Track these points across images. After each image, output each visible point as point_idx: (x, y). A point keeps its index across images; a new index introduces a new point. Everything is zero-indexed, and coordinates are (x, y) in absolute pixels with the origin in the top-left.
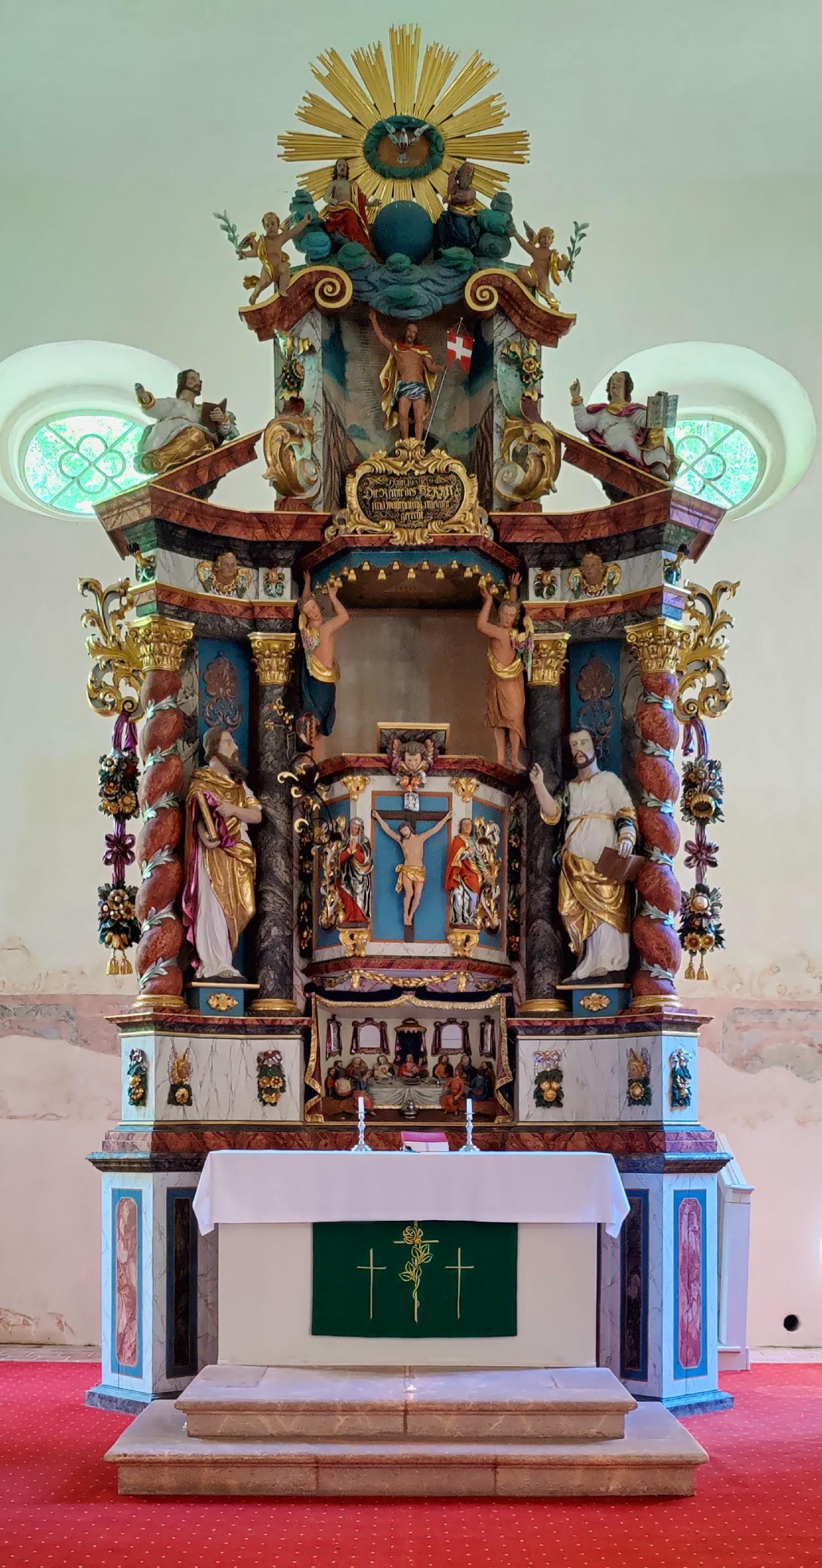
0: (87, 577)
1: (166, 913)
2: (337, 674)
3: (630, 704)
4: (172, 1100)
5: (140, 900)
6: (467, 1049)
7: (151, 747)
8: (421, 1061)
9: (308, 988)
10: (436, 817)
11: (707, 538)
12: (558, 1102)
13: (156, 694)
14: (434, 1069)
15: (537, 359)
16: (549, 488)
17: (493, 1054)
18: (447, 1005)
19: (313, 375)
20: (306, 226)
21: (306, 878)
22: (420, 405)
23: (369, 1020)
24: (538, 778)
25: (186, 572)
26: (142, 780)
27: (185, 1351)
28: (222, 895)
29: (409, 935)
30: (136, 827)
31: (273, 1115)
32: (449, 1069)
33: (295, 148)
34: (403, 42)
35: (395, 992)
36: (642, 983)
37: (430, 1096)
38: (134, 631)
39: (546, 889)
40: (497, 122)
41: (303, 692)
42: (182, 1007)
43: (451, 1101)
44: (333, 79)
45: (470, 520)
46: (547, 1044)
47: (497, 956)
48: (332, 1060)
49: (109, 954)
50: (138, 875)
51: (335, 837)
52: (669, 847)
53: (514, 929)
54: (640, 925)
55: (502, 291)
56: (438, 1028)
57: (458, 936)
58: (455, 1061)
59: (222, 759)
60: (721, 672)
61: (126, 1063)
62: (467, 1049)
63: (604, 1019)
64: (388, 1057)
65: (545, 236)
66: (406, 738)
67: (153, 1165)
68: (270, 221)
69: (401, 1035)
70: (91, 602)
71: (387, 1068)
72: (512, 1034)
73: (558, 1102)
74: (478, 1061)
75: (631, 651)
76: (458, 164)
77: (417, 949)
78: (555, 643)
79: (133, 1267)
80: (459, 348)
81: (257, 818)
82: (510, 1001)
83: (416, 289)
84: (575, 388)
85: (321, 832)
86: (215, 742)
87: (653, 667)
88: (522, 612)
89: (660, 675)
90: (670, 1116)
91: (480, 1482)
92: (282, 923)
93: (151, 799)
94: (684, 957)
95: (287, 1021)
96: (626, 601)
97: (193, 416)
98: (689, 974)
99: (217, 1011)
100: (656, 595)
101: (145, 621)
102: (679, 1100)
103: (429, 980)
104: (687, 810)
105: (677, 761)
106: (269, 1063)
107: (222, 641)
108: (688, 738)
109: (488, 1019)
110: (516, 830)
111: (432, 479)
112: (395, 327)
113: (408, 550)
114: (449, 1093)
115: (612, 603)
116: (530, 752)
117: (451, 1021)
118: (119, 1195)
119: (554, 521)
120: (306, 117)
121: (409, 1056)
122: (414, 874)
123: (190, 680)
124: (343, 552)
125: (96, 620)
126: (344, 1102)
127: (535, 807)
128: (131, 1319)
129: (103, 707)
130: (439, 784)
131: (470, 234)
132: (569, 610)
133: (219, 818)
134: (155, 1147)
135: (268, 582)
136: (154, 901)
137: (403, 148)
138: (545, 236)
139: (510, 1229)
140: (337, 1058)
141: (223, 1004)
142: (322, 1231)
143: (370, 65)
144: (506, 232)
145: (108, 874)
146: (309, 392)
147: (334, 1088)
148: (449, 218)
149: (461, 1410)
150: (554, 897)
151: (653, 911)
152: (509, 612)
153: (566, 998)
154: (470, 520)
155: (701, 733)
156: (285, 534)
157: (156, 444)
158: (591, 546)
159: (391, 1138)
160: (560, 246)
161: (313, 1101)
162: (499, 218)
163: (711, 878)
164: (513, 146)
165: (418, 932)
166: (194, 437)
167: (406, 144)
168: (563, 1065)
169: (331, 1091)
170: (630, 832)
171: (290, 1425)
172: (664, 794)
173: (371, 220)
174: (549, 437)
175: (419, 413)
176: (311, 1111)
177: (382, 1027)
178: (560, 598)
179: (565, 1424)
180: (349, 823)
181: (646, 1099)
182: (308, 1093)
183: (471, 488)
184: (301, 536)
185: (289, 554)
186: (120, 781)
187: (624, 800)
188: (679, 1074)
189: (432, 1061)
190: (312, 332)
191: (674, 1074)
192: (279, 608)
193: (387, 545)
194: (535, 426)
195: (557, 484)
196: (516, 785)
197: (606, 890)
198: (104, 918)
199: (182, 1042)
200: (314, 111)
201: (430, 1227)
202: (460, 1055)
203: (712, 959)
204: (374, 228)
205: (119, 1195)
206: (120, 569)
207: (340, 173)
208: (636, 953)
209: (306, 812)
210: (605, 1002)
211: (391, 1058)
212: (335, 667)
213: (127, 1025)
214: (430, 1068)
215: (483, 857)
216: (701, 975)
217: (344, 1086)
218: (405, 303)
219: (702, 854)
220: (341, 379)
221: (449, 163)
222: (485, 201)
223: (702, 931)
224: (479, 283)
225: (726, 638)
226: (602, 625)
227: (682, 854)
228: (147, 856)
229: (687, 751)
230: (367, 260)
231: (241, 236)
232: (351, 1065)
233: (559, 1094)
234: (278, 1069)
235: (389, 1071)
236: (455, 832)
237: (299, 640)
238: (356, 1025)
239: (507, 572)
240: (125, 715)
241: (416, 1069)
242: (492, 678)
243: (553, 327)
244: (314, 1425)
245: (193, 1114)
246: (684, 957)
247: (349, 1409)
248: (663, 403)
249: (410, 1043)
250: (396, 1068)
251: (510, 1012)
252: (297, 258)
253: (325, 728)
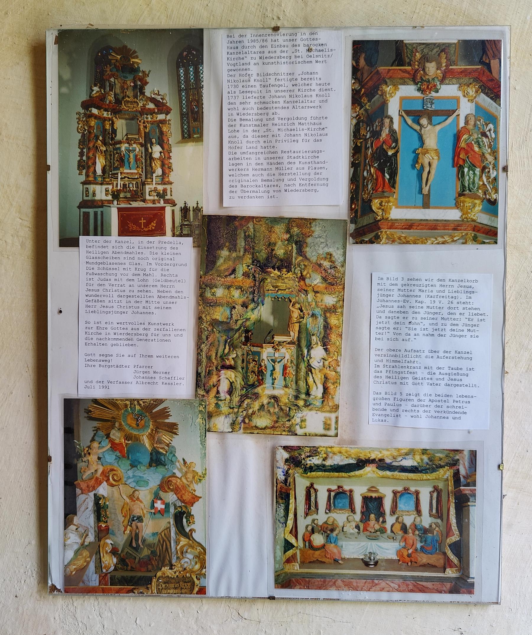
8: (381, 519)
14: (392, 526)
37: (387, 549)
43: (405, 554)
48: (309, 519)
64: (355, 516)
71: (354, 524)
114: (404, 548)
121: (372, 516)
126: (317, 553)
140: (315, 516)
147: (310, 542)
159: (355, 584)
161: (290, 553)
202: (413, 517)
211: (358, 517)
214: (388, 526)
217: (318, 540)
232: (326, 523)
235: (356, 527)
241: (377, 527)
250: (362, 526)
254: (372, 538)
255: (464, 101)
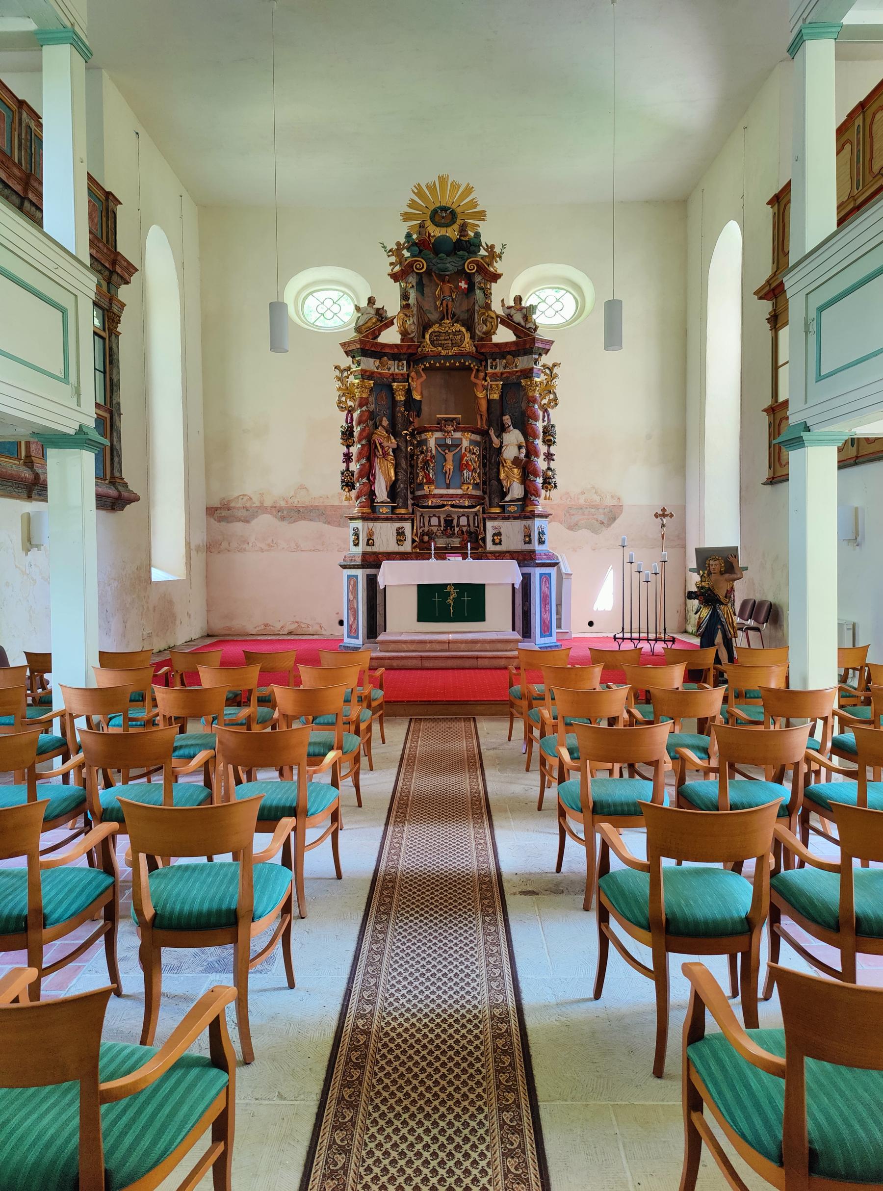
0: (336, 364)
1: (365, 480)
2: (422, 397)
3: (523, 405)
4: (368, 544)
5: (356, 475)
6: (469, 525)
7: (359, 424)
9: (413, 505)
10: (458, 446)
11: (549, 350)
12: (500, 543)
13: (361, 406)
15: (490, 289)
16: (494, 333)
17: (478, 527)
18: (462, 510)
19: (413, 294)
20: (411, 244)
21: (412, 466)
22: (450, 303)
23: (434, 515)
24: (492, 432)
25: (370, 364)
26: (356, 434)
27: (373, 630)
28: (384, 474)
29: (448, 487)
30: (354, 450)
31: (402, 549)
32: (462, 532)
33: (406, 217)
34: (443, 180)
35: (443, 506)
36: (528, 502)
37: (456, 542)
38: (354, 384)
39: (495, 470)
40: (475, 208)
41: (411, 404)
42: (371, 513)
44: (419, 193)
45: (468, 345)
46: (496, 523)
47: (478, 493)
49: (345, 493)
50: (354, 467)
51: (422, 453)
52: (537, 456)
53: (484, 483)
54: (527, 482)
55: (478, 265)
56: (459, 518)
57: (465, 487)
58: (464, 529)
59: (383, 427)
60: (555, 394)
61: (352, 532)
62: (469, 525)
63: (517, 515)
65: (493, 247)
66: (446, 420)
67: (362, 567)
68: (398, 244)
69: (445, 520)
70: (338, 373)
72: (484, 520)
73: (500, 543)
74: (473, 529)
75: (524, 389)
76: (462, 222)
77: (451, 491)
78: (497, 385)
79: (355, 601)
80: (463, 285)
81: (395, 446)
82: (483, 508)
83: (448, 265)
84: (503, 301)
85: (417, 451)
86: (381, 421)
87: (531, 394)
88: (486, 375)
89: (533, 397)
90: (538, 548)
91: (473, 663)
92: (404, 483)
93: (359, 441)
94: (543, 492)
95: (406, 516)
96: (521, 371)
97: (373, 312)
98: (545, 498)
99: (382, 513)
100: (532, 369)
101: (357, 381)
102: (541, 542)
103: (456, 502)
104: (544, 441)
105: (540, 425)
106: (400, 531)
107: (381, 386)
108: (544, 417)
109: (476, 514)
110: (485, 449)
111: (454, 334)
112: (442, 278)
113: (447, 357)
115: (517, 372)
116: (490, 423)
117: (463, 515)
118: (350, 577)
119: (497, 345)
120: (410, 206)
122: (449, 466)
123: (372, 399)
124: (425, 357)
125: (339, 379)
127: (491, 442)
128: (354, 619)
129: (342, 409)
130: (458, 435)
131: (467, 246)
132: (502, 374)
133: (383, 447)
134: (363, 560)
135: (398, 366)
136: (361, 476)
137: (443, 217)
138: (493, 247)
139: (483, 586)
141: (384, 510)
142: (421, 587)
143: (432, 188)
144: (480, 244)
145: (343, 466)
146: (412, 301)
148: (459, 240)
149: (466, 642)
150: (498, 473)
151: (532, 477)
152: (482, 374)
153: (503, 507)
154: (468, 345)
155: (548, 415)
156: (404, 351)
157: (361, 323)
158: (509, 353)
160: (497, 250)
162: (476, 241)
163: (553, 465)
164: (481, 215)
165: (451, 486)
166: (374, 320)
167: (444, 215)
168: (502, 531)
169: (422, 540)
170: (524, 450)
171: (412, 647)
172: (535, 437)
173: (433, 240)
174: (494, 316)
175: (450, 306)
176: (414, 548)
177: (439, 517)
178: (499, 370)
179: (499, 646)
180: (427, 449)
181: (530, 542)
182: (413, 541)
183: (467, 336)
184: (409, 351)
185: (406, 356)
186: (347, 435)
187: (521, 439)
188: (541, 533)
189: (457, 529)
190: (412, 280)
191: (539, 533)
192: (402, 374)
193: (439, 354)
194: (490, 312)
195: (497, 332)
196: (484, 434)
197: (516, 470)
198: (343, 481)
199: (371, 524)
200: (413, 204)
201: (456, 586)
203: (554, 493)
204: (433, 244)
205: (349, 577)
206: (347, 361)
207: (422, 226)
208: (526, 492)
209: (412, 444)
210: (516, 509)
212: (422, 394)
213: (352, 519)
215: (472, 459)
216: (549, 499)
217: (426, 538)
218: (446, 270)
219: (549, 457)
220: (423, 294)
221: (459, 222)
222: (472, 234)
223: (549, 484)
224: (470, 263)
225: (556, 382)
226: (513, 379)
227: (542, 457)
228: (358, 461)
229: (544, 421)
230: (432, 256)
231: (388, 249)
233: (501, 540)
234: (403, 533)
236: (463, 451)
237: (409, 385)
238: (430, 517)
239: (481, 361)
240: (349, 411)
242: (476, 397)
243: (495, 277)
244: (420, 647)
245: (375, 549)
246: (543, 492)
247: (431, 642)
248: (532, 309)
249: (449, 523)
251: (484, 513)
252: (406, 254)
253: (418, 415)
254: (448, 537)
255: (464, 440)
